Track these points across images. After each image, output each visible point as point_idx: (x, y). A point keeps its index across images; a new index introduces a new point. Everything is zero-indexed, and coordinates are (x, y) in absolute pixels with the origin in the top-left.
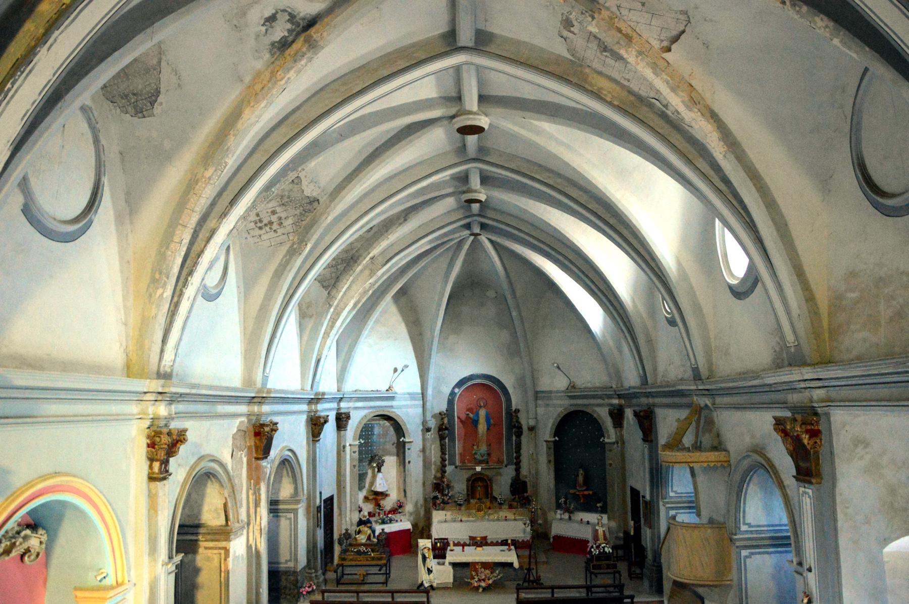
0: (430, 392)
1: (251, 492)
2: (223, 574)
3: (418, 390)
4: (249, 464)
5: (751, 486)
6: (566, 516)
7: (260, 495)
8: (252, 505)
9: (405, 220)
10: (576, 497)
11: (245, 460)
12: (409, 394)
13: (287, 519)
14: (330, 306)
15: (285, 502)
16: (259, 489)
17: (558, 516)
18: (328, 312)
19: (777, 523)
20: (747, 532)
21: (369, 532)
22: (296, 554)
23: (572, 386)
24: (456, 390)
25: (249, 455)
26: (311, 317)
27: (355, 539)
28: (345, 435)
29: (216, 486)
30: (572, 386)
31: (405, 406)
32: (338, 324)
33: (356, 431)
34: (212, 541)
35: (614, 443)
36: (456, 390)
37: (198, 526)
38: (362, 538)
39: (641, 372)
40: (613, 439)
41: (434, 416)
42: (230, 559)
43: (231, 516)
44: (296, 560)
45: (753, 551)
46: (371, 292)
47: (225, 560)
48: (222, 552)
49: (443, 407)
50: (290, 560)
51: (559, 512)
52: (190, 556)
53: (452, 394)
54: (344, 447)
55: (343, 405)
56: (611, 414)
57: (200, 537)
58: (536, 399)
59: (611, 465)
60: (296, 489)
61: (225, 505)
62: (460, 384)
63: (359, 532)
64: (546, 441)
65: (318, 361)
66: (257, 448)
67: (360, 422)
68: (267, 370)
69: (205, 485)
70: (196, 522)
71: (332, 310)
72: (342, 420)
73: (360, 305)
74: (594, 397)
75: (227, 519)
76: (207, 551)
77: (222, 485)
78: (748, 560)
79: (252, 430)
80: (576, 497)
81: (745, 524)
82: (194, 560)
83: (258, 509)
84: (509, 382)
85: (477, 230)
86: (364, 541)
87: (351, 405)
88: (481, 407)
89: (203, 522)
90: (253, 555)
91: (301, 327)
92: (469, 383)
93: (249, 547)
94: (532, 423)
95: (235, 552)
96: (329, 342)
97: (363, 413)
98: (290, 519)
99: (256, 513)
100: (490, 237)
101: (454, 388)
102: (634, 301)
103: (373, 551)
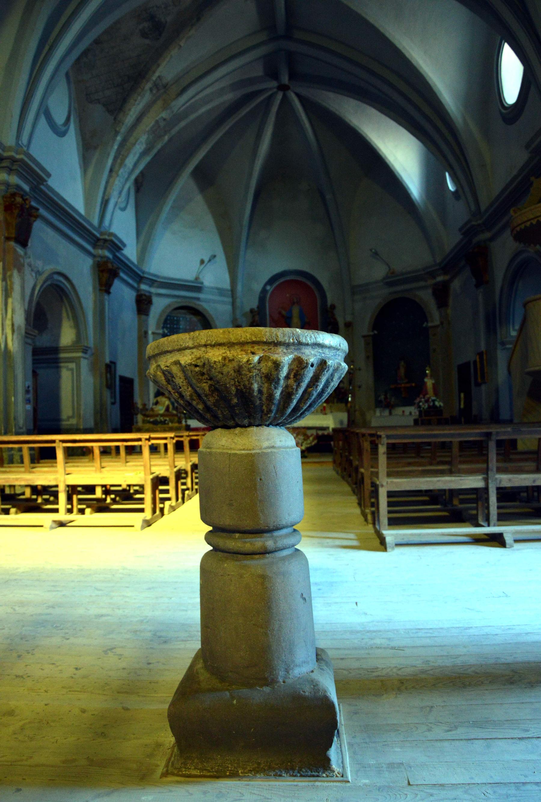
0: (239, 288)
3: (226, 284)
6: (387, 412)
7: (12, 283)
12: (218, 289)
13: (68, 369)
14: (117, 133)
15: (67, 349)
16: (11, 276)
17: (378, 414)
18: (114, 140)
21: (167, 402)
22: (79, 409)
23: (392, 273)
24: (268, 288)
26: (95, 148)
27: (152, 410)
28: (147, 321)
30: (392, 273)
31: (214, 301)
32: (130, 161)
33: (159, 320)
36: (268, 288)
38: (161, 409)
39: (473, 208)
40: (437, 323)
41: (245, 315)
44: (79, 416)
46: (166, 138)
49: (254, 304)
50: (72, 417)
53: (264, 291)
54: (146, 333)
55: (143, 287)
58: (353, 293)
59: (434, 350)
62: (271, 281)
63: (157, 403)
64: (364, 337)
65: (105, 203)
66: (8, 224)
67: (163, 311)
68: (25, 139)
71: (119, 138)
72: (143, 304)
73: (155, 151)
74: (416, 279)
83: (10, 300)
85: (285, 79)
87: (153, 290)
88: (293, 303)
92: (282, 280)
94: (349, 318)
96: (117, 183)
97: (167, 301)
98: (72, 370)
100: (299, 90)
102: (465, 120)
103: (172, 422)
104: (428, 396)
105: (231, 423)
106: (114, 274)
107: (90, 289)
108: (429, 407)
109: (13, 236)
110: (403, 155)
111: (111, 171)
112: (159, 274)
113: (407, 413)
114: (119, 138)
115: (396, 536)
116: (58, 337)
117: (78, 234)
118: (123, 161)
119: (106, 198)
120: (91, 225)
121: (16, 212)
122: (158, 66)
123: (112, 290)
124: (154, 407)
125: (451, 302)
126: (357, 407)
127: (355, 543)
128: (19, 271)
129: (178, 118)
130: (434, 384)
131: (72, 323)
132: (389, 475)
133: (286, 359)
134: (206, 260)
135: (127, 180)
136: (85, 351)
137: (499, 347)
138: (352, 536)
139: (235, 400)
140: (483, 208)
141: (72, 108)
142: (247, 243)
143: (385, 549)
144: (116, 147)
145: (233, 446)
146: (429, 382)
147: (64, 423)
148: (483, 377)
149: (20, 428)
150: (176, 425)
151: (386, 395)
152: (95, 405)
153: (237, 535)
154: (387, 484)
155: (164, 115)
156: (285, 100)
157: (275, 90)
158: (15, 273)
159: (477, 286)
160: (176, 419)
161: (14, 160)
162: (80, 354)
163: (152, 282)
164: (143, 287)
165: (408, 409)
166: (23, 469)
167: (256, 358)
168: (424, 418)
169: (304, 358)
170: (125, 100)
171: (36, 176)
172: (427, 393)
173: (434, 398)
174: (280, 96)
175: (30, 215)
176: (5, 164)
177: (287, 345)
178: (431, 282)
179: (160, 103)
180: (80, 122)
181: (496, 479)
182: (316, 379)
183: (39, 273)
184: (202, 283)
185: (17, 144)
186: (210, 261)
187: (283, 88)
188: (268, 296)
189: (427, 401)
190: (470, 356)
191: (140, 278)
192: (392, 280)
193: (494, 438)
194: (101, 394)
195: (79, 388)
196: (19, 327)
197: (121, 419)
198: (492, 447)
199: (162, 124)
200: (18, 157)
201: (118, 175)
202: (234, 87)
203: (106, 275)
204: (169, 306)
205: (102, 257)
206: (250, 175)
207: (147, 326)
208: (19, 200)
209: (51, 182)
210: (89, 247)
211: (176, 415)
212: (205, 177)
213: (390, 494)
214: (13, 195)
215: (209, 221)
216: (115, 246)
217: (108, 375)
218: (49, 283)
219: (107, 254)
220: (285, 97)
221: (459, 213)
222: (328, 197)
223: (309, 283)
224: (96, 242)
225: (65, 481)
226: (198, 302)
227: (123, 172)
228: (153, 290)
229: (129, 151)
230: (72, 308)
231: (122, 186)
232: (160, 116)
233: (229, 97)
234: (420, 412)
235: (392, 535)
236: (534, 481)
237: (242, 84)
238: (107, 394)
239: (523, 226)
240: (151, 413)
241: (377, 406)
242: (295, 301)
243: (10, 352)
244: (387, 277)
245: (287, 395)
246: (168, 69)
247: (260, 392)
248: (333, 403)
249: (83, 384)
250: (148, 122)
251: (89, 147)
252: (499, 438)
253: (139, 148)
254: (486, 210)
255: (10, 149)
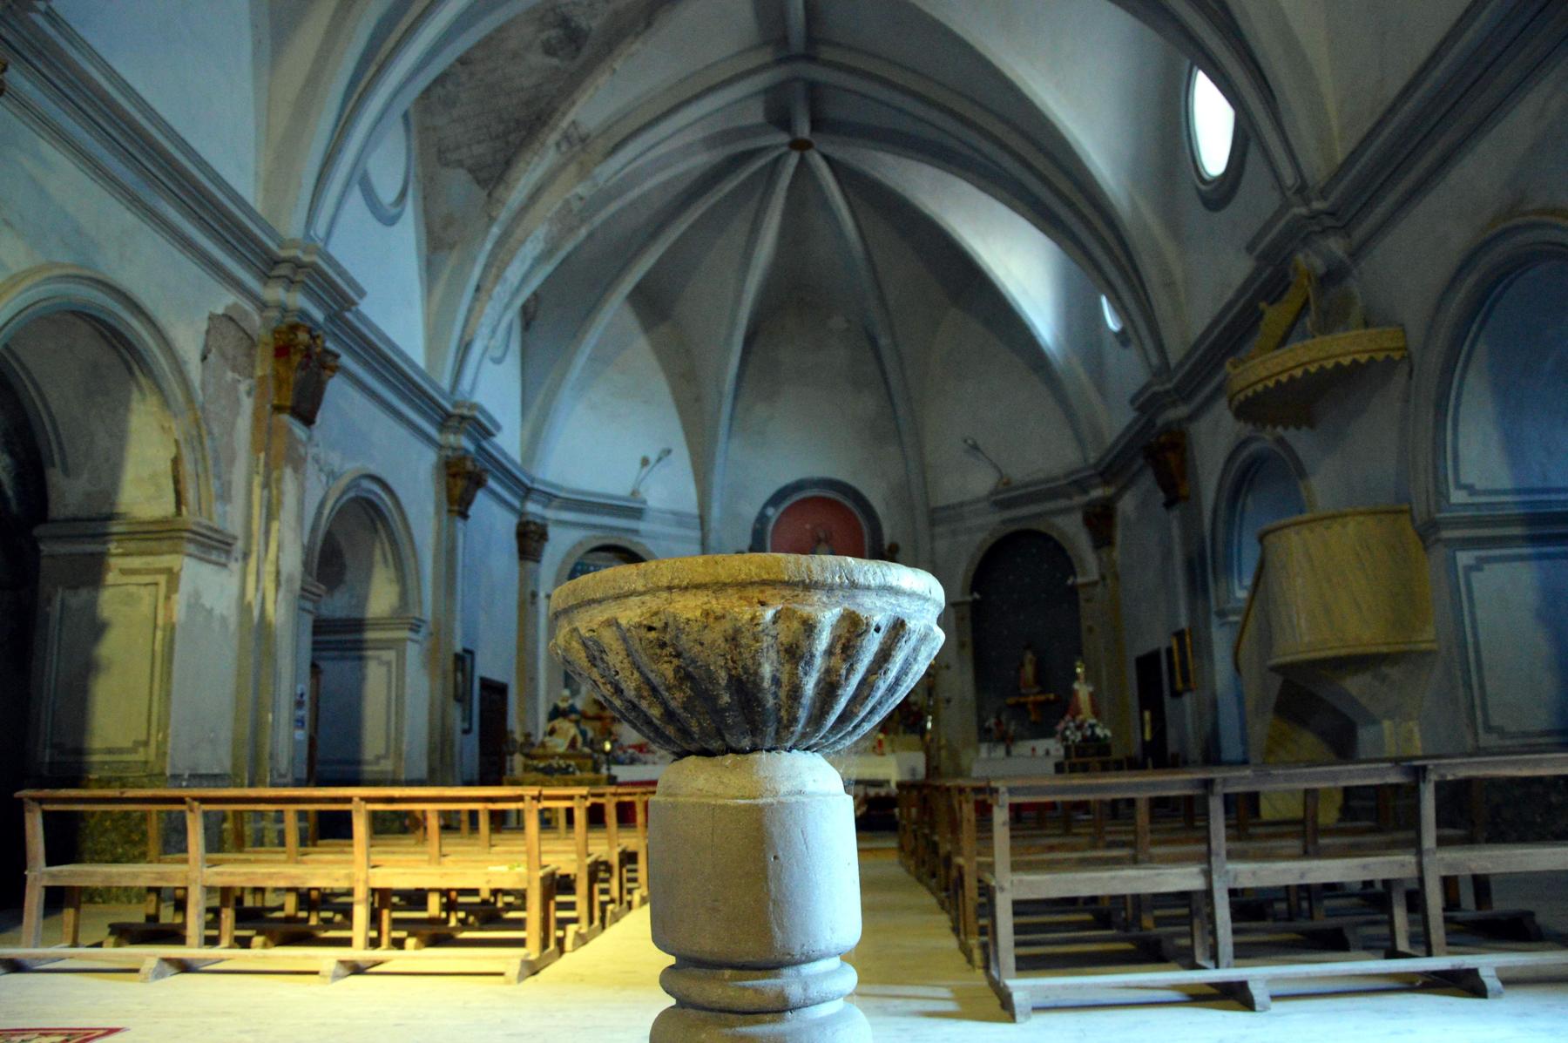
0: (716, 512)
1: (258, 480)
2: (159, 634)
4: (257, 417)
5: (1471, 378)
6: (1000, 751)
7: (281, 493)
8: (256, 510)
9: (649, 25)
10: (1020, 709)
11: (247, 404)
12: (674, 513)
13: (381, 662)
14: (492, 220)
15: (380, 624)
16: (280, 480)
19: (1539, 484)
20: (1466, 506)
21: (573, 731)
22: (398, 740)
23: (1006, 484)
24: (770, 511)
25: (258, 391)
26: (452, 247)
27: (543, 745)
29: (153, 401)
30: (1006, 484)
32: (514, 272)
34: (142, 553)
35: (1095, 583)
36: (770, 511)
37: (111, 517)
38: (560, 744)
39: (1155, 360)
40: (1094, 575)
42: (180, 601)
43: (190, 495)
44: (399, 755)
45: (1483, 553)
46: (583, 232)
47: (168, 598)
48: (162, 579)
50: (385, 757)
51: (984, 748)
52: (84, 593)
53: (762, 518)
54: (534, 595)
56: (1088, 521)
57: (113, 547)
58: (933, 523)
59: (1090, 630)
60: (403, 595)
61: (176, 462)
62: (775, 500)
63: (552, 732)
65: (465, 348)
66: (280, 382)
67: (569, 554)
69: (127, 409)
70: (105, 510)
71: (496, 230)
72: (530, 539)
73: (562, 254)
74: (1054, 494)
75: (179, 500)
76: (125, 579)
77: (166, 402)
78: (1475, 576)
79: (268, 338)
80: (1021, 706)
81: (1460, 486)
82: (92, 605)
83: (275, 526)
84: (876, 496)
85: (804, 130)
86: (561, 750)
87: (550, 514)
89: (122, 509)
90: (261, 633)
91: (430, 269)
92: (796, 497)
93: (244, 608)
95: (197, 595)
96: (490, 310)
97: (575, 535)
98: (388, 664)
99: (267, 532)
100: (829, 150)
101: (766, 505)
104: (1081, 717)
105: (715, 744)
106: (477, 481)
107: (431, 509)
108: (1085, 739)
109: (289, 404)
110: (1023, 267)
111: (478, 289)
112: (565, 484)
113: (1040, 752)
114: (496, 230)
115: (1033, 991)
116: (363, 601)
117: (410, 402)
118: (502, 270)
119: (467, 338)
120: (438, 388)
121: (296, 359)
122: (574, 103)
123: (472, 511)
124: (547, 739)
125: (1119, 536)
126: (943, 742)
127: (951, 1006)
128: (296, 470)
129: (607, 196)
130: (1092, 696)
131: (391, 573)
132: (1016, 867)
133: (828, 618)
134: (653, 457)
135: (507, 307)
136: (415, 628)
137: (1215, 620)
138: (943, 992)
139: (726, 698)
140: (1173, 362)
141: (412, 178)
142: (730, 430)
143: (1012, 1018)
144: (488, 246)
145: (720, 790)
146: (1083, 691)
147: (367, 768)
148: (1186, 679)
149: (281, 776)
150: (590, 775)
151: (998, 718)
152: (431, 735)
153: (728, 973)
154: (1013, 886)
155: (582, 189)
156: (803, 167)
157: (785, 149)
158: (288, 472)
159: (1169, 504)
160: (590, 763)
161: (298, 265)
162: (406, 634)
163: (549, 498)
164: (532, 508)
165: (1042, 745)
166: (283, 857)
167: (769, 614)
168: (1074, 760)
169: (863, 614)
170: (508, 164)
171: (339, 297)
172: (1078, 712)
173: (1093, 721)
174: (794, 158)
175: (324, 366)
176: (283, 270)
177: (830, 589)
178: (1079, 500)
179: (573, 168)
180: (425, 198)
181: (1227, 872)
182: (884, 656)
183: (332, 475)
184: (645, 502)
185: (307, 235)
186: (659, 460)
187: (800, 145)
188: (770, 527)
189: (1079, 727)
190: (1156, 638)
191: (526, 492)
192: (1005, 497)
193: (1219, 789)
194: (444, 711)
195: (400, 698)
196: (290, 580)
197: (481, 764)
198: (1216, 806)
199: (576, 206)
200: (306, 259)
201: (490, 297)
202: (711, 142)
203: (461, 483)
204: (581, 544)
205: (454, 449)
206: (738, 301)
207: (536, 581)
208: (303, 337)
209: (365, 307)
210: (432, 431)
211: (590, 757)
212: (654, 305)
213: (1020, 907)
214: (294, 328)
215: (660, 385)
216: (480, 428)
217: (459, 675)
218: (352, 494)
219: (466, 443)
220: (803, 161)
221: (1130, 372)
222: (884, 341)
223: (848, 504)
224: (445, 420)
225: (367, 881)
226: (636, 539)
227: (501, 292)
228: (550, 514)
229: (512, 254)
230: (394, 542)
231: (498, 318)
232: (573, 192)
233: (702, 160)
234: (1067, 748)
235: (1024, 988)
236: (1302, 875)
237: (725, 137)
238: (456, 713)
239: (1250, 392)
240: (541, 751)
241: (981, 740)
242: (822, 535)
243: (270, 625)
244: (995, 492)
245: (829, 690)
246: (593, 107)
247: (776, 681)
248: (896, 733)
249: (408, 691)
250: (551, 203)
251: (439, 242)
252: (1229, 790)
253: (531, 249)
254: (1181, 365)
255: (294, 243)
